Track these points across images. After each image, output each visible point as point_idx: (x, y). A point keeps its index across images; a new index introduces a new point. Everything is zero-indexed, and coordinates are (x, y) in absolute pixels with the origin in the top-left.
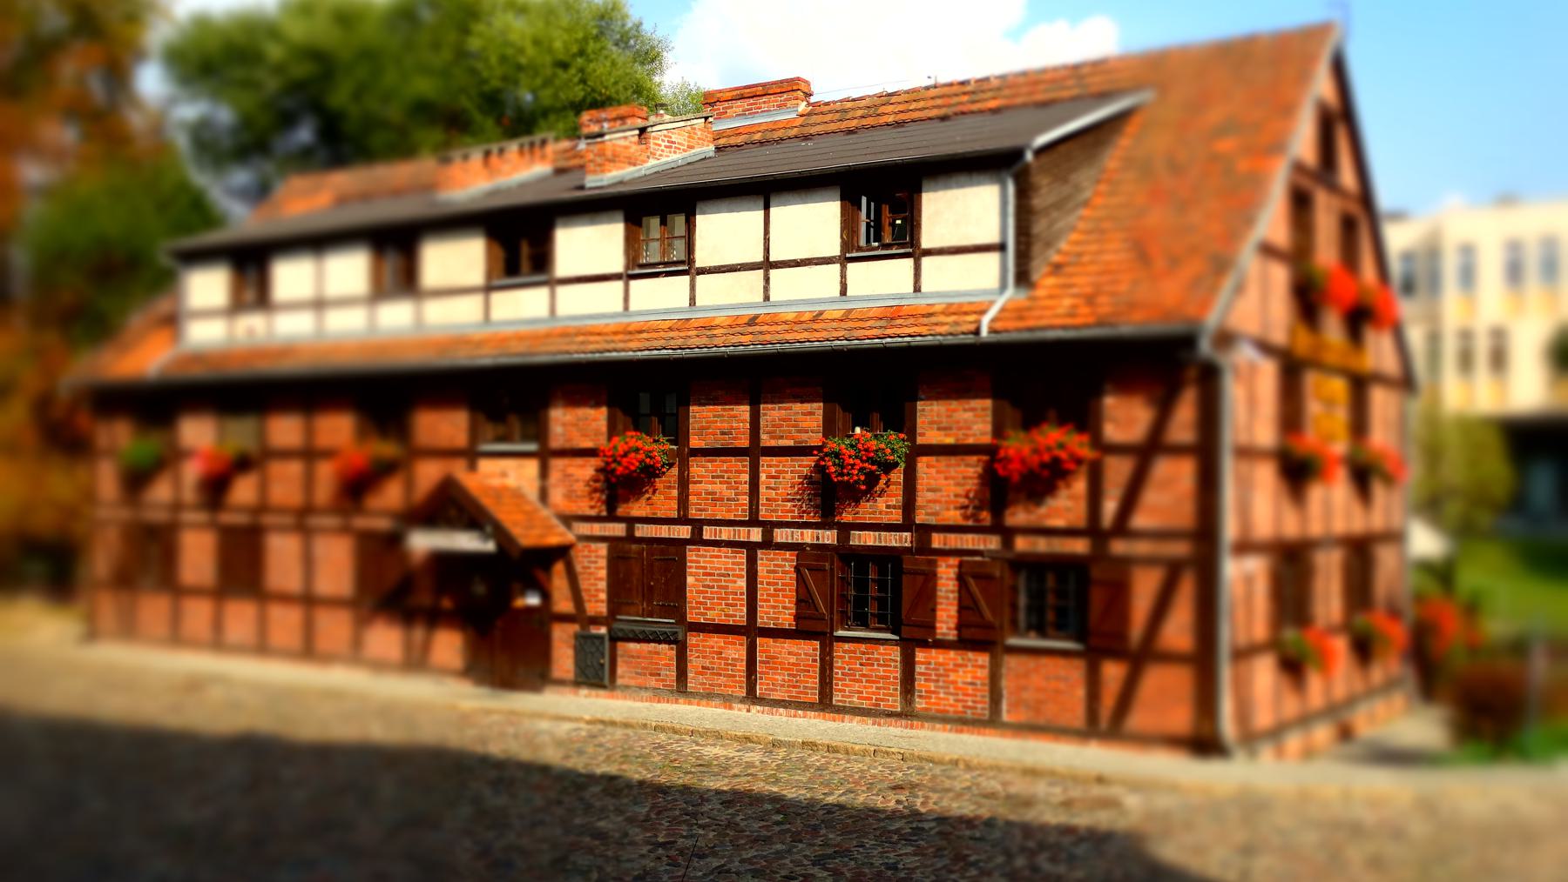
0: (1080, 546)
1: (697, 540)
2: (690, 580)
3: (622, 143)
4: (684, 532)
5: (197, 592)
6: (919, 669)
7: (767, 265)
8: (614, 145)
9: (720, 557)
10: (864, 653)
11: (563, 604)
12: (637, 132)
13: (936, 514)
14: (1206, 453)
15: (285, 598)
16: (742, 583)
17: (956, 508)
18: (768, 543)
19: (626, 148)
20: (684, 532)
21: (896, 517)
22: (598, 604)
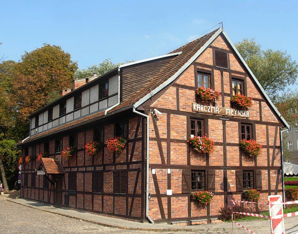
0: (125, 167)
1: (78, 172)
2: (77, 181)
3: (81, 82)
4: (76, 170)
5: (29, 188)
6: (104, 201)
7: (90, 105)
8: (77, 83)
9: (80, 175)
10: (97, 197)
11: (64, 188)
12: (85, 79)
13: (106, 161)
14: (143, 140)
15: (37, 188)
16: (83, 181)
17: (109, 159)
18: (86, 171)
19: (82, 83)
20: (76, 170)
21: (101, 163)
22: (67, 188)
